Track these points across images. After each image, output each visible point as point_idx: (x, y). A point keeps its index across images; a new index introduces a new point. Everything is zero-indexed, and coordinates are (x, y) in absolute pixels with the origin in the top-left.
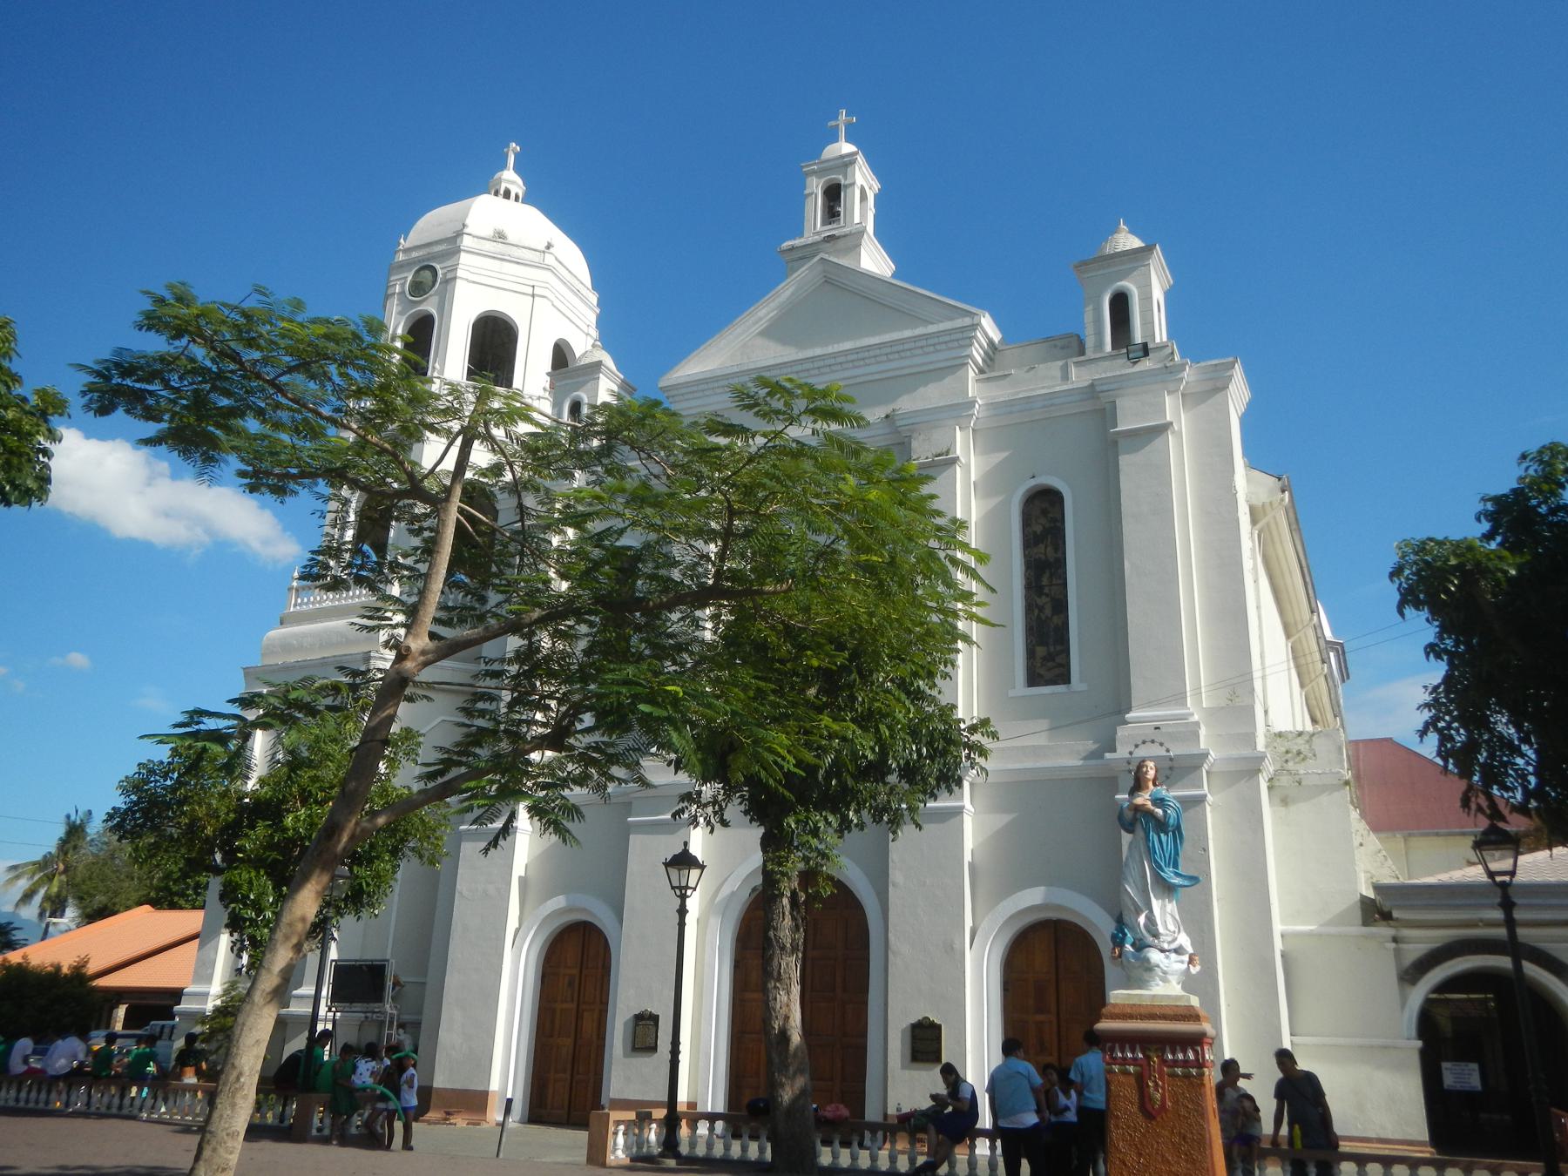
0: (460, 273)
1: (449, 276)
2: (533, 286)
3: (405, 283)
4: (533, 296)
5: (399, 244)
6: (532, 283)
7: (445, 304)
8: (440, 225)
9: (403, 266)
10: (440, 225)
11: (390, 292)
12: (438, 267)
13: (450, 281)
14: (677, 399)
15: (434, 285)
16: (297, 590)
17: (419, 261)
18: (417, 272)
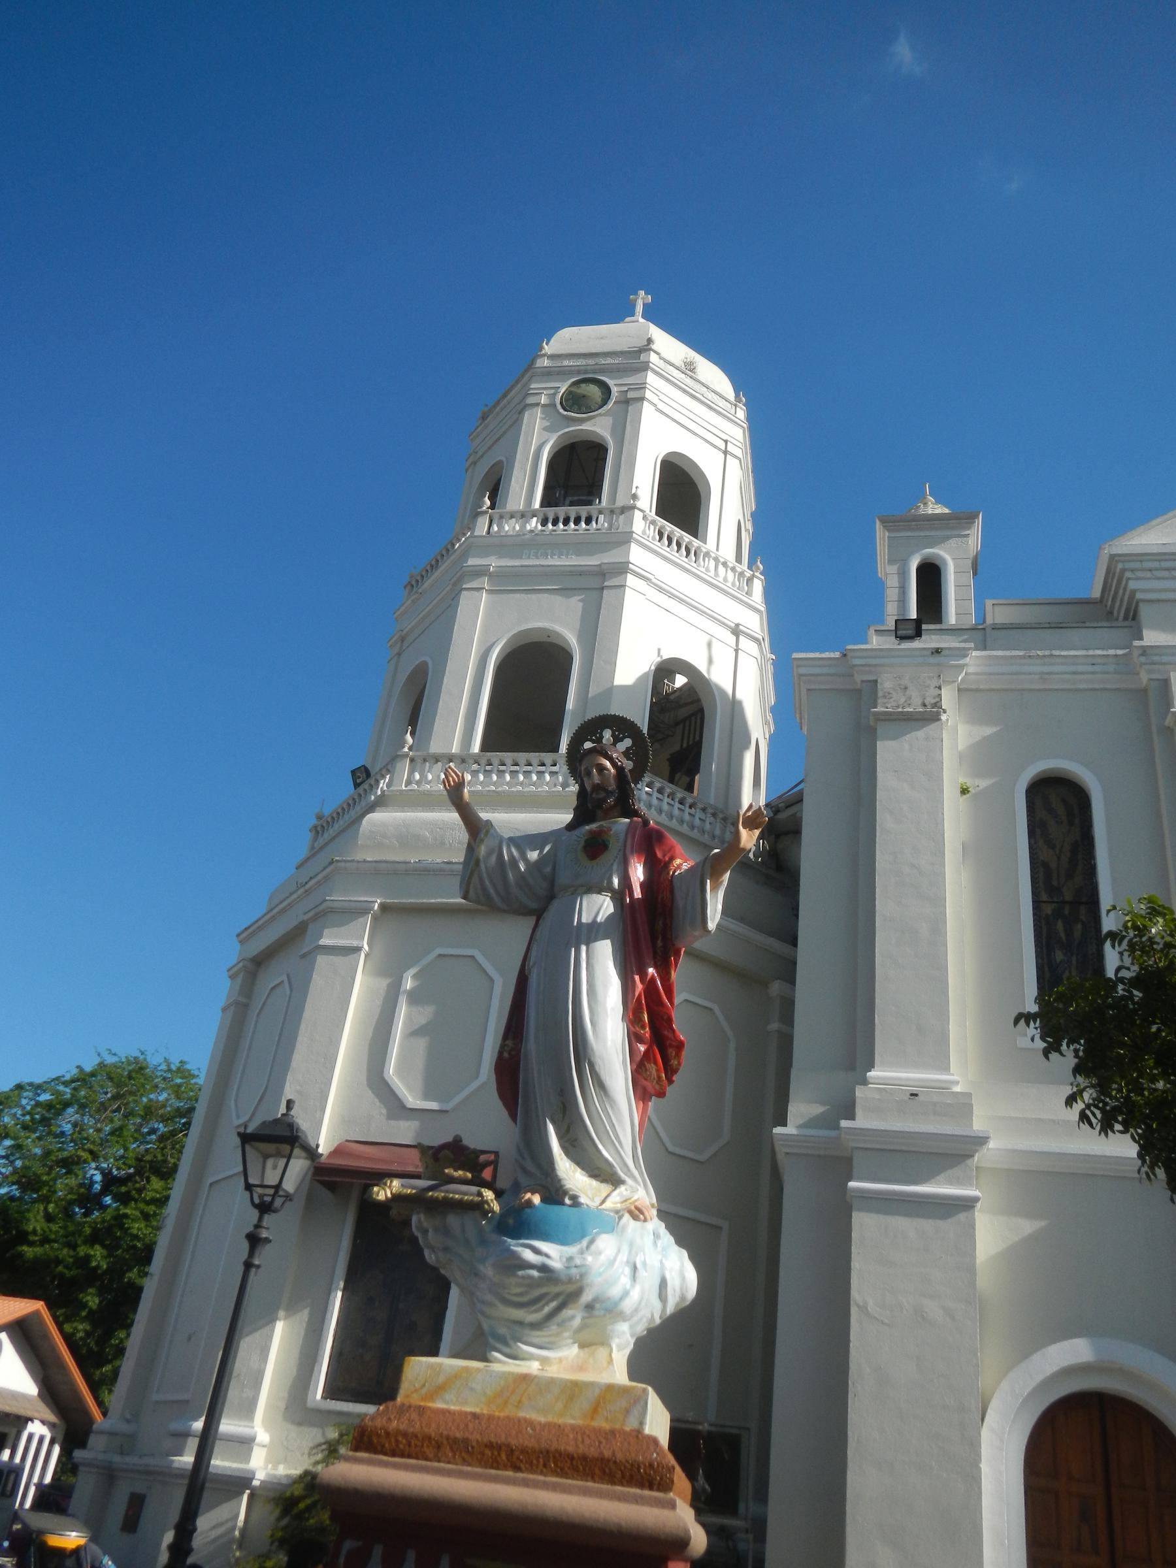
0: (648, 394)
1: (631, 395)
2: (726, 442)
3: (555, 394)
4: (726, 452)
5: (542, 348)
6: (725, 437)
7: (626, 426)
8: (602, 338)
9: (548, 374)
10: (602, 338)
11: (531, 400)
12: (611, 382)
13: (632, 401)
14: (1139, 574)
15: (605, 401)
16: (412, 760)
17: (579, 372)
18: (574, 384)
